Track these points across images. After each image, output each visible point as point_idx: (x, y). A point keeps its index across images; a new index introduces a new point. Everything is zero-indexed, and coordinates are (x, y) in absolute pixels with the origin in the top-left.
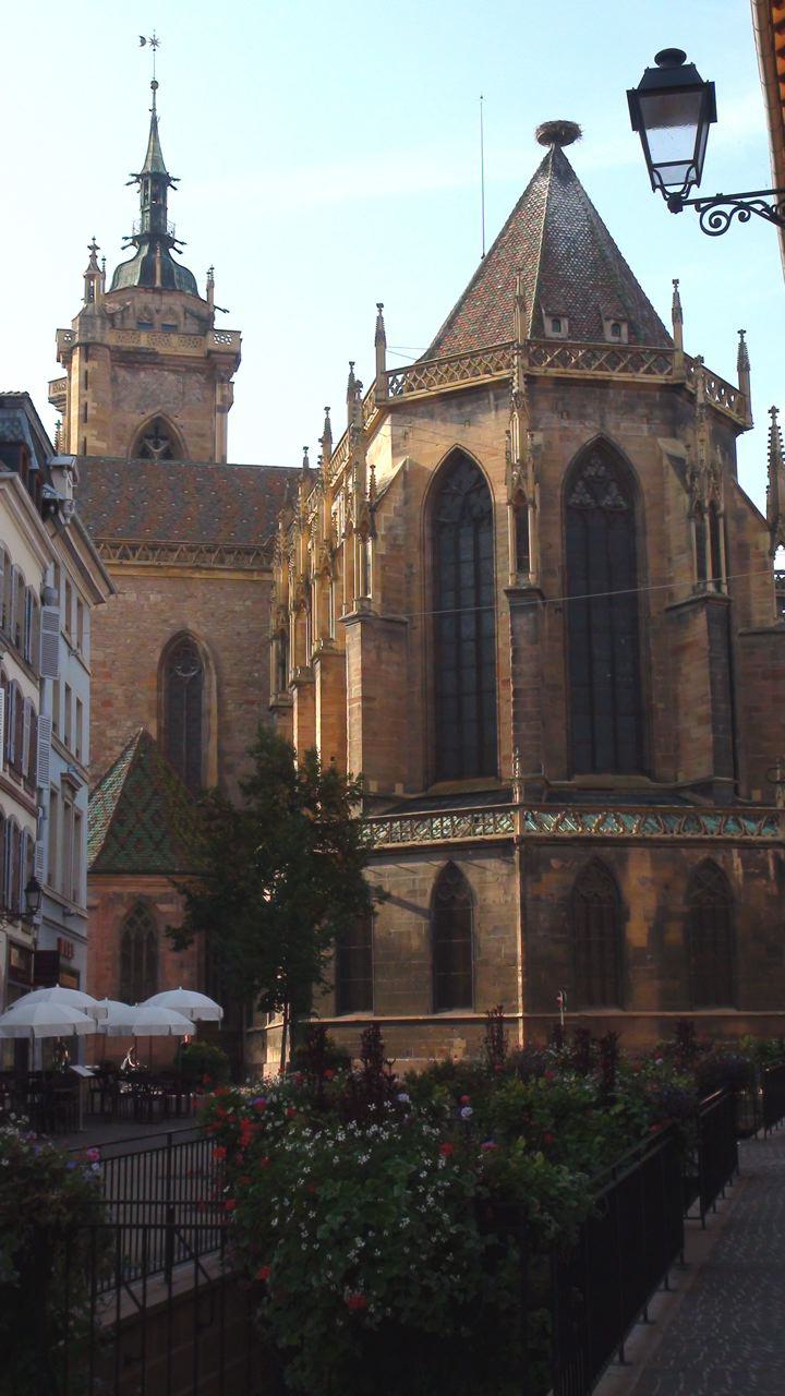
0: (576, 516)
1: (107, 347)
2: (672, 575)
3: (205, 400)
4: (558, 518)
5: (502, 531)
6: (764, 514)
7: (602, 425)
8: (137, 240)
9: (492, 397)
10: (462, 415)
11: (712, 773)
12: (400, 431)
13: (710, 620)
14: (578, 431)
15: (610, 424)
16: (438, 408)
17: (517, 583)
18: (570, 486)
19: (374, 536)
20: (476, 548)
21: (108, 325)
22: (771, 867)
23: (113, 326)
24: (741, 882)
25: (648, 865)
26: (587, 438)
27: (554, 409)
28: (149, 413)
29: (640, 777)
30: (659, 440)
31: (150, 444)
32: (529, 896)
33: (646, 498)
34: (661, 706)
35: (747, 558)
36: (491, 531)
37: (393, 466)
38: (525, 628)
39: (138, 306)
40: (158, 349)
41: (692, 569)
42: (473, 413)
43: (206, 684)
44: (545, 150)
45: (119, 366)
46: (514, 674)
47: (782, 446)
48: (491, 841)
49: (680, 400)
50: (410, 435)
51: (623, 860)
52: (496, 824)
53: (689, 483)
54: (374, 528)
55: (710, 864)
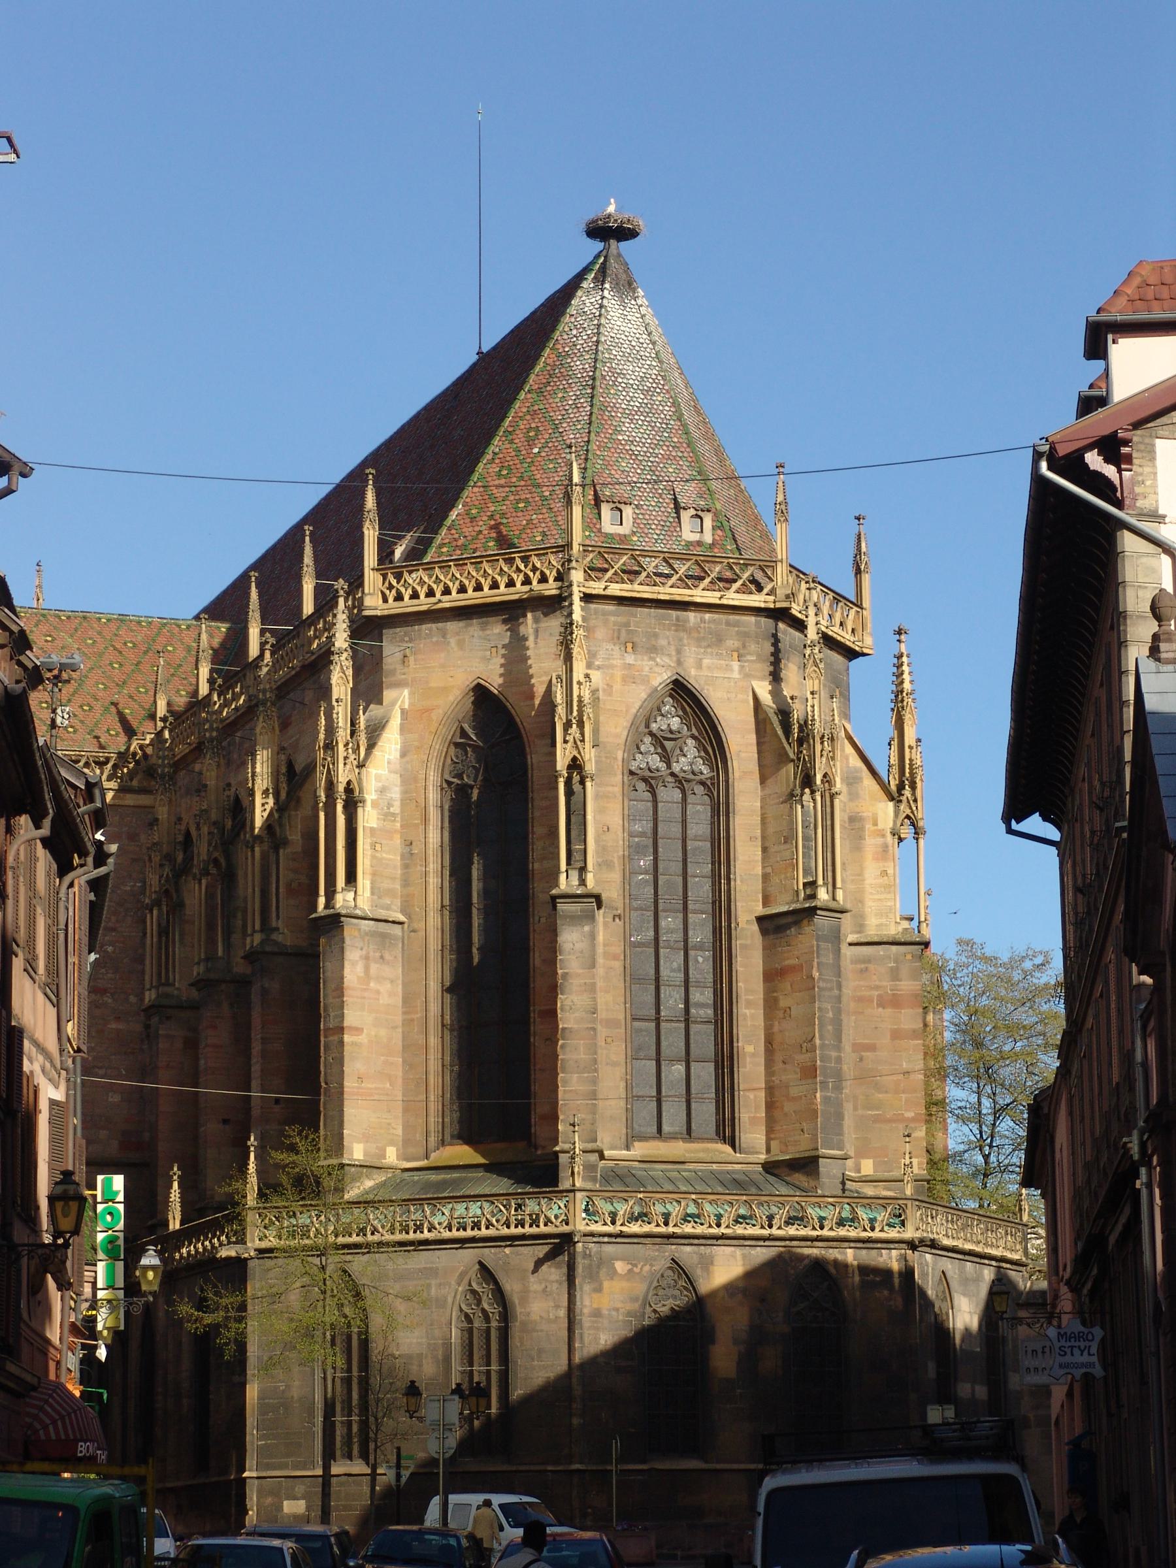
4: (617, 790)
7: (679, 663)
14: (647, 669)
16: (452, 626)
24: (858, 1293)
27: (616, 638)
35: (861, 838)
36: (526, 801)
38: (579, 946)
50: (412, 659)
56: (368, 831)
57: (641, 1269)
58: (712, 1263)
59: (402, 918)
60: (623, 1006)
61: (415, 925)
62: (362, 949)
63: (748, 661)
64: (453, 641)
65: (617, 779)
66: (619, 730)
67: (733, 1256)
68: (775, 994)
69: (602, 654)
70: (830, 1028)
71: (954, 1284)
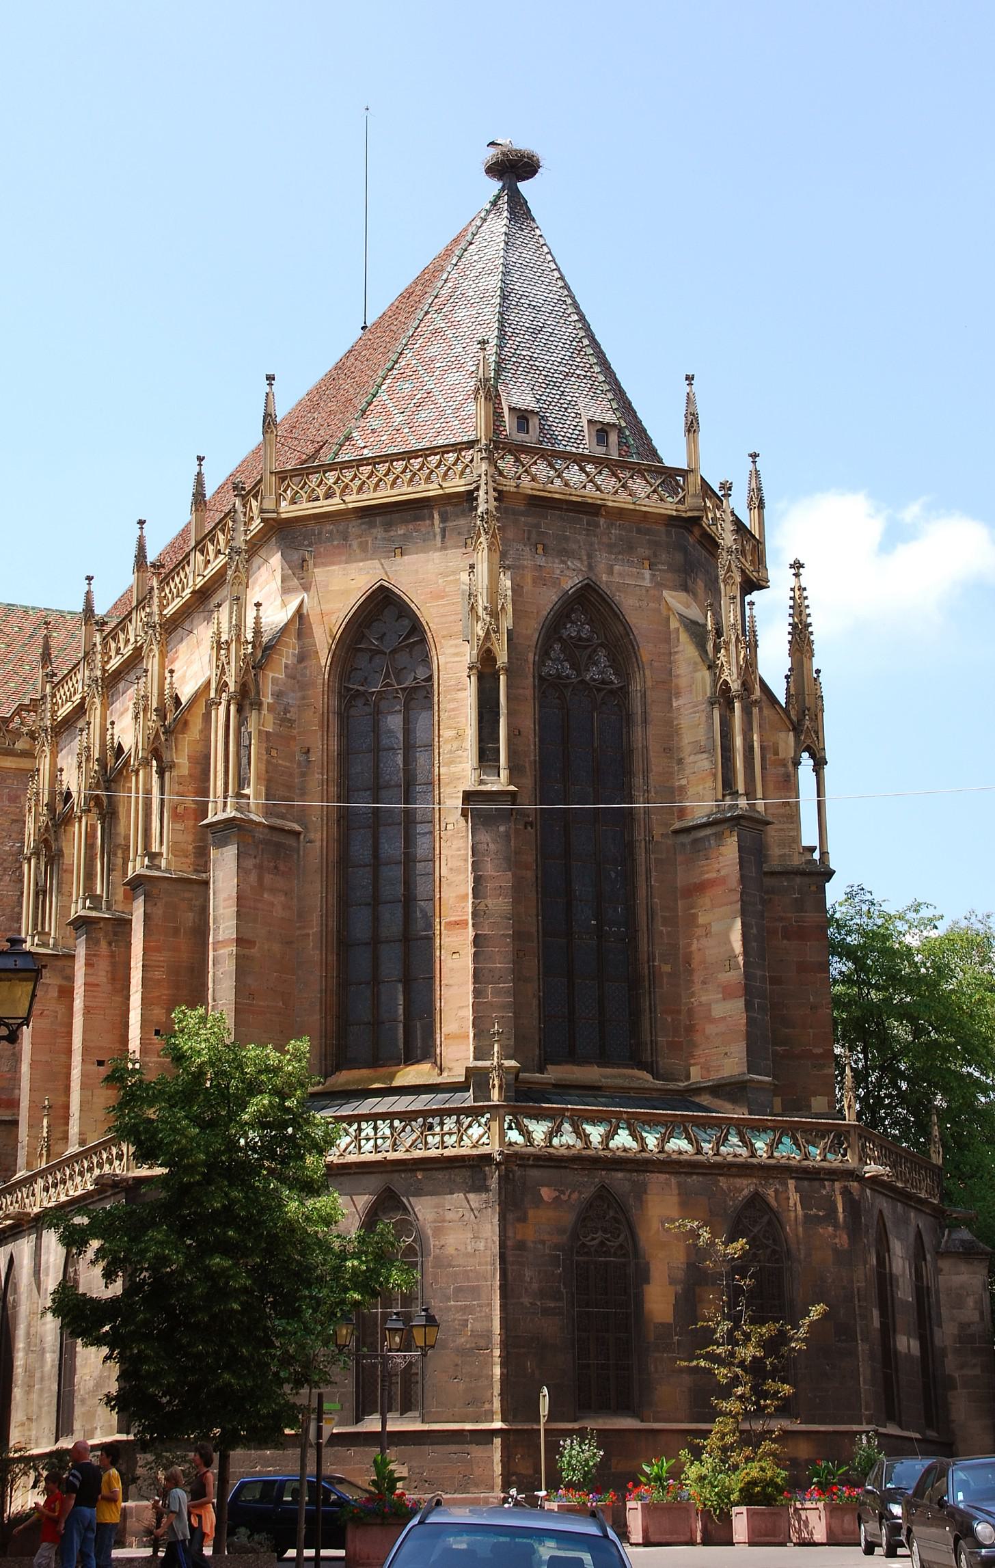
0: (548, 687)
2: (684, 782)
4: (529, 693)
5: (452, 706)
7: (590, 567)
9: (436, 516)
10: (390, 540)
11: (745, 1070)
12: (296, 556)
13: (741, 849)
14: (558, 572)
15: (601, 567)
16: (354, 528)
18: (544, 652)
19: (258, 705)
20: (408, 731)
22: (840, 1209)
24: (801, 1229)
25: (675, 1199)
26: (570, 584)
29: (636, 1072)
32: (509, 1243)
33: (647, 673)
34: (666, 968)
37: (284, 604)
41: (715, 775)
42: (406, 537)
46: (475, 914)
47: (809, 615)
50: (311, 563)
51: (640, 1191)
52: (461, 1133)
53: (711, 656)
54: (258, 693)
55: (757, 1200)
56: (264, 735)
57: (569, 1196)
58: (645, 1192)
59: (297, 827)
60: (535, 918)
61: (312, 836)
62: (255, 857)
63: (660, 570)
64: (355, 544)
66: (529, 632)
68: (693, 911)
70: (754, 944)
71: (889, 1224)
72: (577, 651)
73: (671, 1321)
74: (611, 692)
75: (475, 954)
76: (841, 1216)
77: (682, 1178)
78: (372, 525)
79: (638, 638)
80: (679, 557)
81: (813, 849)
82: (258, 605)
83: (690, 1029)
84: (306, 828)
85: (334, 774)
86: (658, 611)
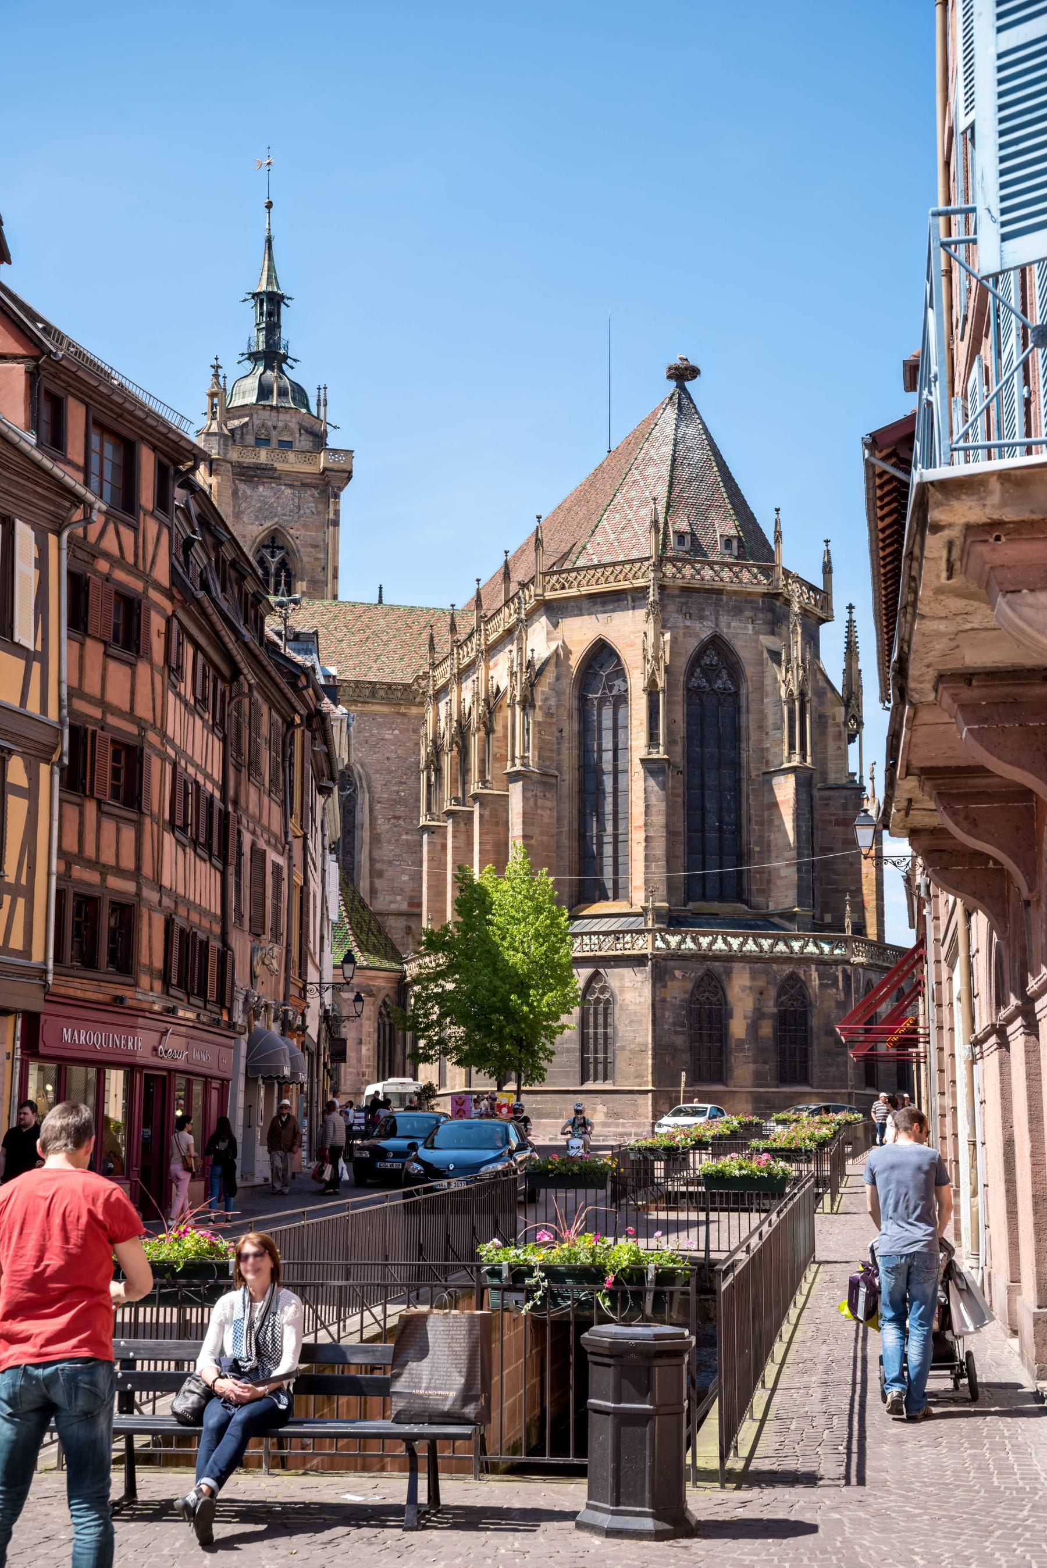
0: (692, 693)
1: (231, 463)
3: (319, 513)
6: (840, 692)
7: (717, 625)
8: (253, 357)
9: (630, 598)
12: (554, 621)
16: (585, 604)
17: (649, 753)
18: (690, 673)
19: (533, 706)
21: (230, 442)
22: (840, 979)
23: (234, 441)
25: (748, 976)
27: (679, 611)
28: (267, 524)
29: (739, 905)
30: (761, 637)
31: (266, 553)
33: (750, 683)
39: (257, 422)
40: (276, 465)
43: (359, 801)
44: (673, 384)
45: (240, 480)
48: (629, 956)
49: (778, 603)
51: (729, 972)
54: (533, 700)
55: (793, 977)
59: (556, 773)
65: (680, 695)
67: (744, 968)
69: (672, 620)
72: (710, 673)
73: (744, 1037)
74: (730, 694)
75: (646, 847)
76: (841, 984)
77: (752, 965)
78: (595, 604)
79: (745, 664)
80: (769, 616)
81: (854, 774)
82: (532, 650)
83: (769, 882)
84: (561, 773)
85: (575, 743)
86: (756, 647)
